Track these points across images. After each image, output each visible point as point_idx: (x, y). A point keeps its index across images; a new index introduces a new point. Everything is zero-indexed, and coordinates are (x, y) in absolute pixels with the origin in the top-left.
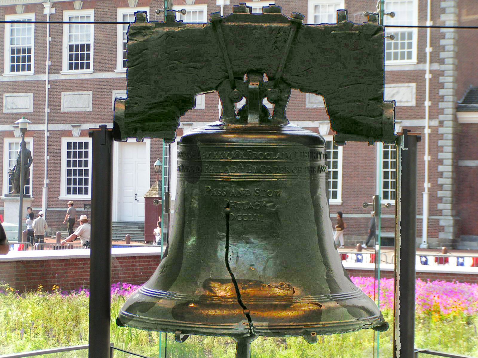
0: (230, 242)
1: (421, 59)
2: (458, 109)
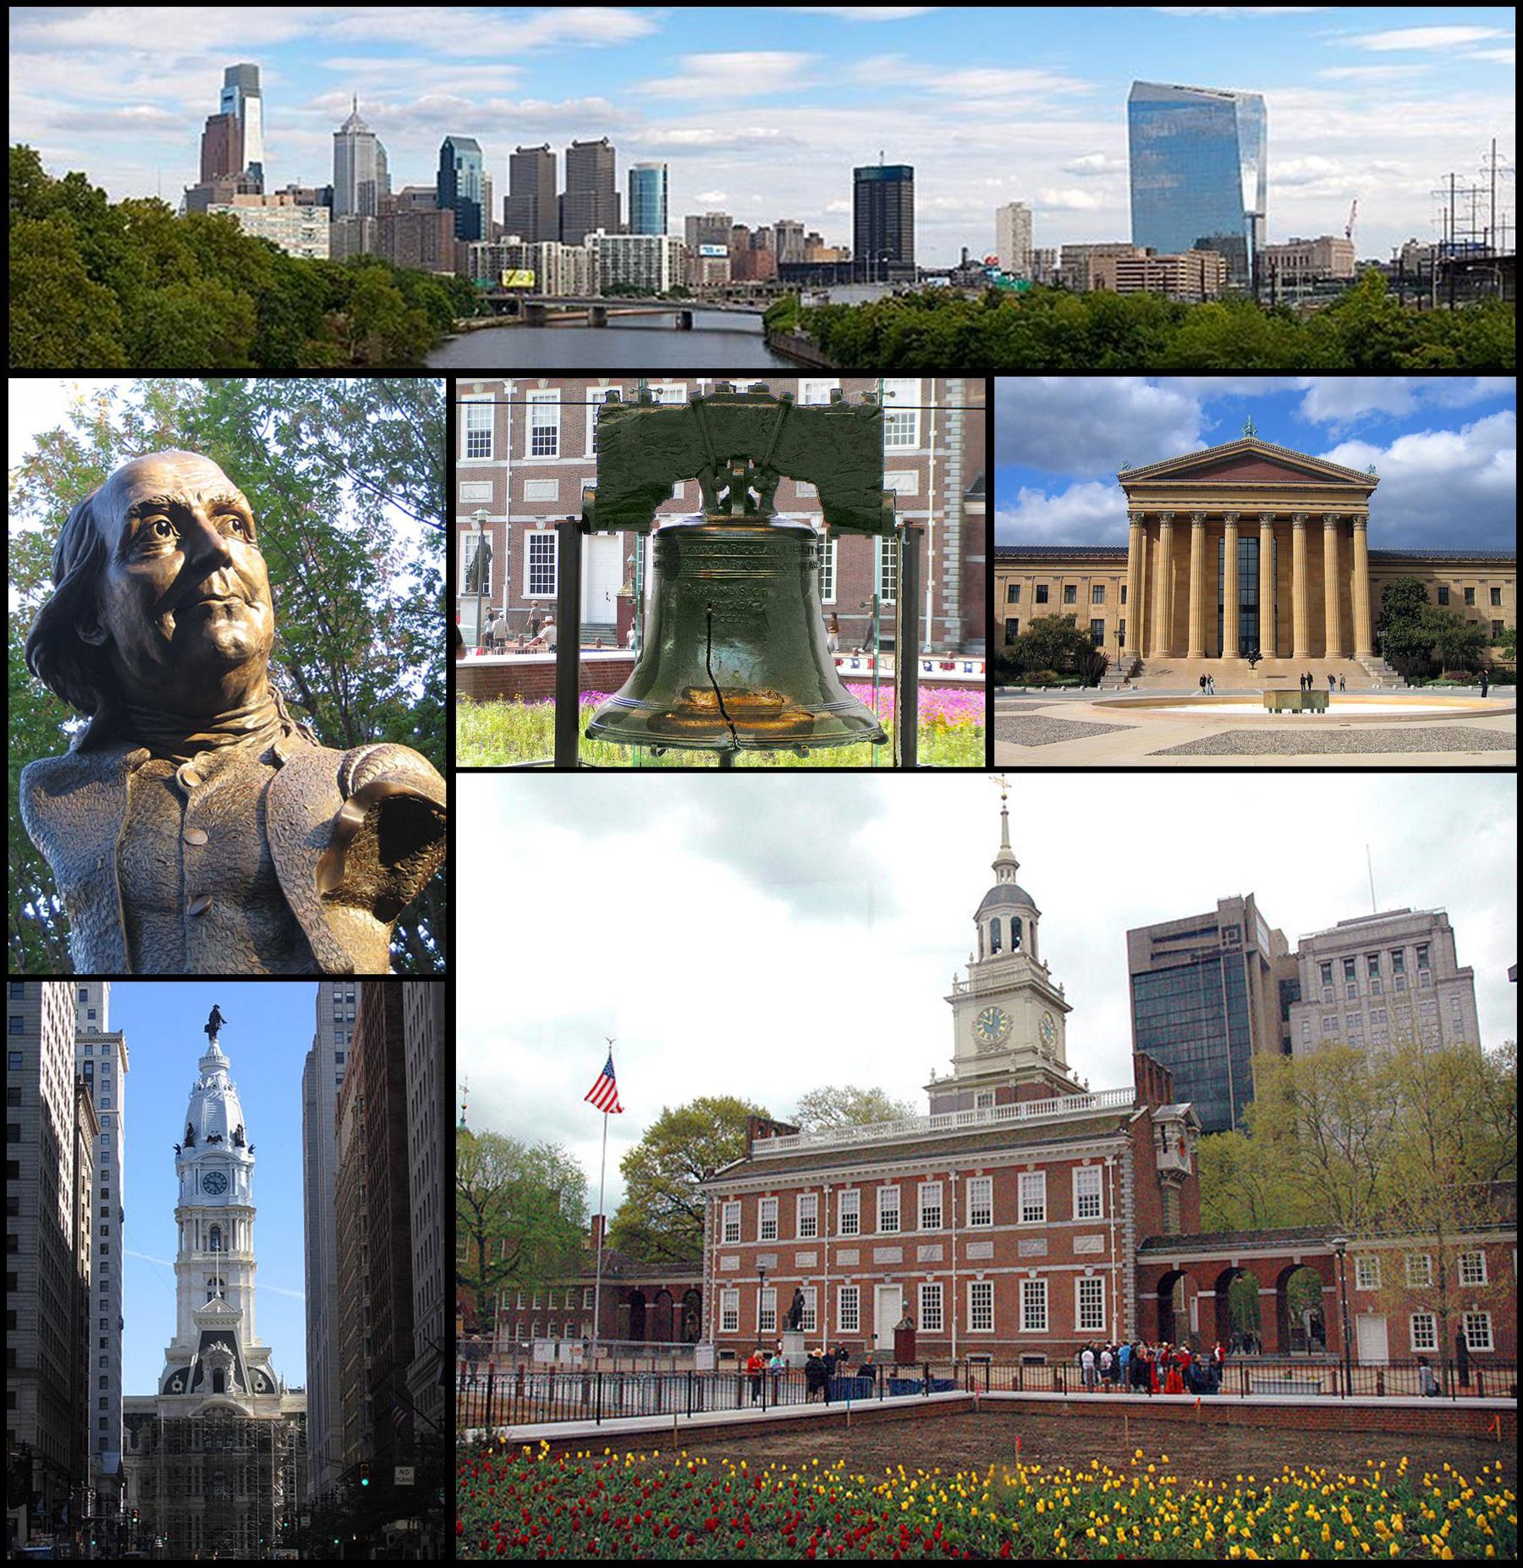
1: (1107, 1215)
2: (1137, 1253)
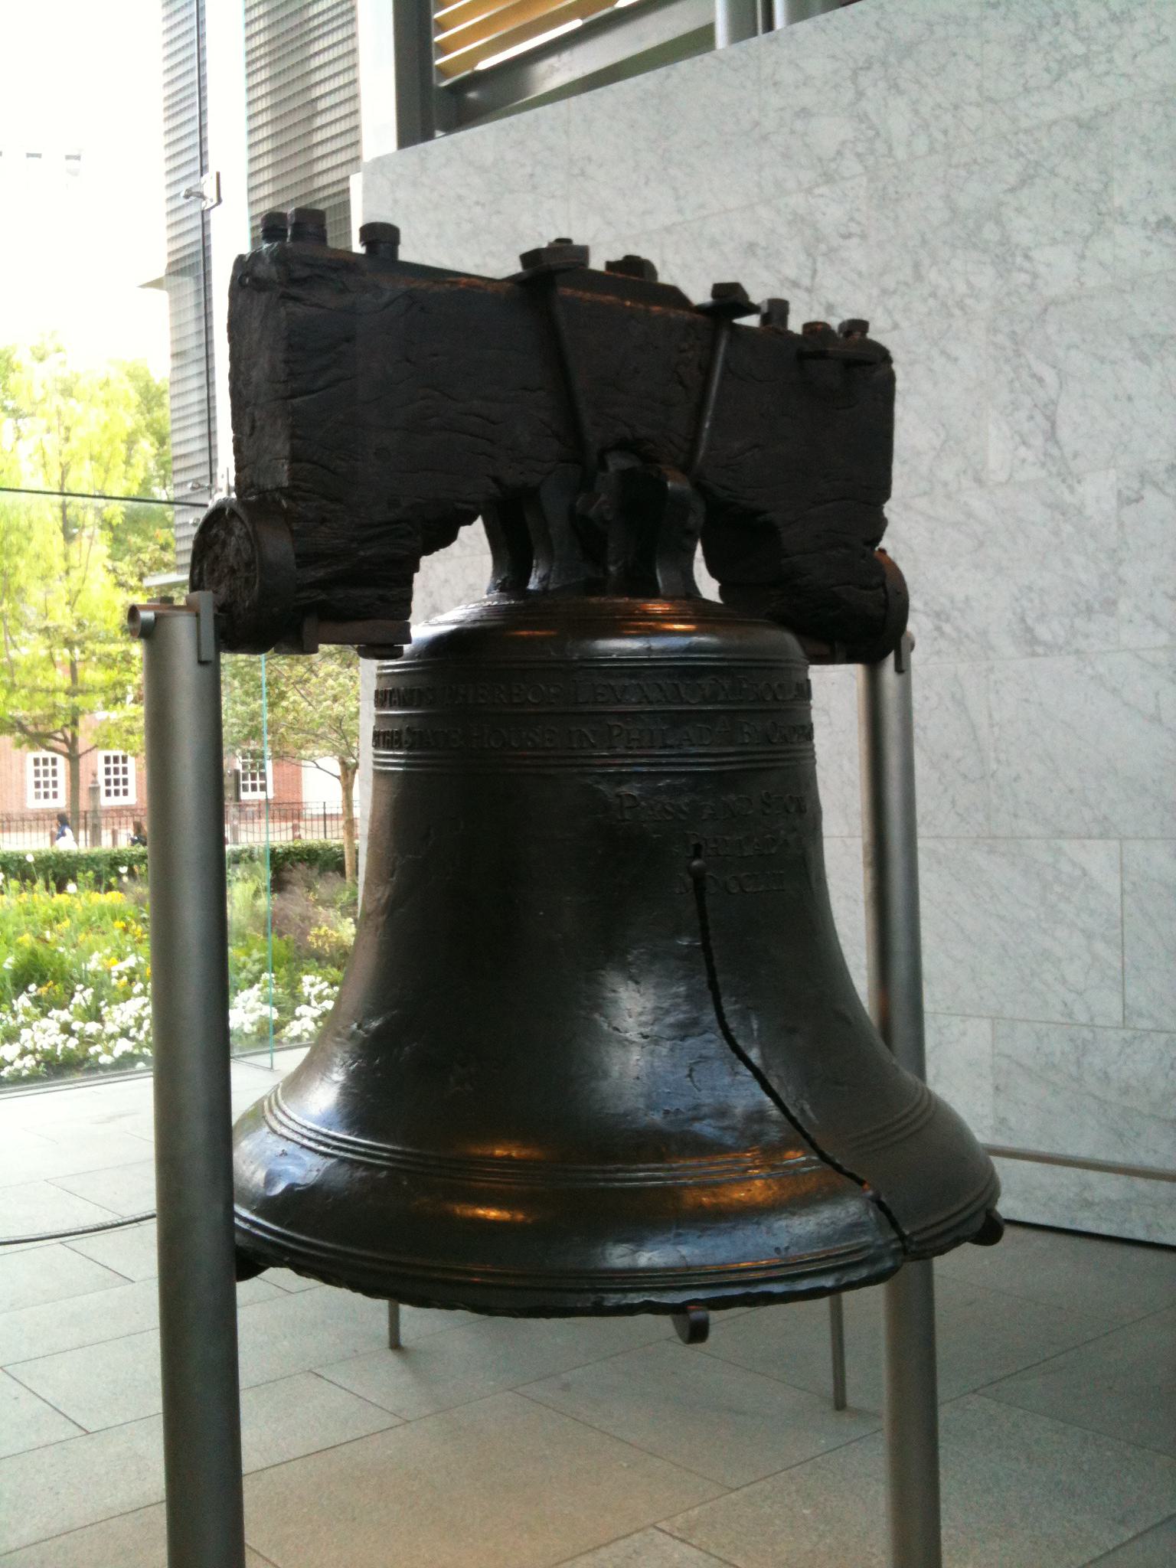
0: (716, 963)
